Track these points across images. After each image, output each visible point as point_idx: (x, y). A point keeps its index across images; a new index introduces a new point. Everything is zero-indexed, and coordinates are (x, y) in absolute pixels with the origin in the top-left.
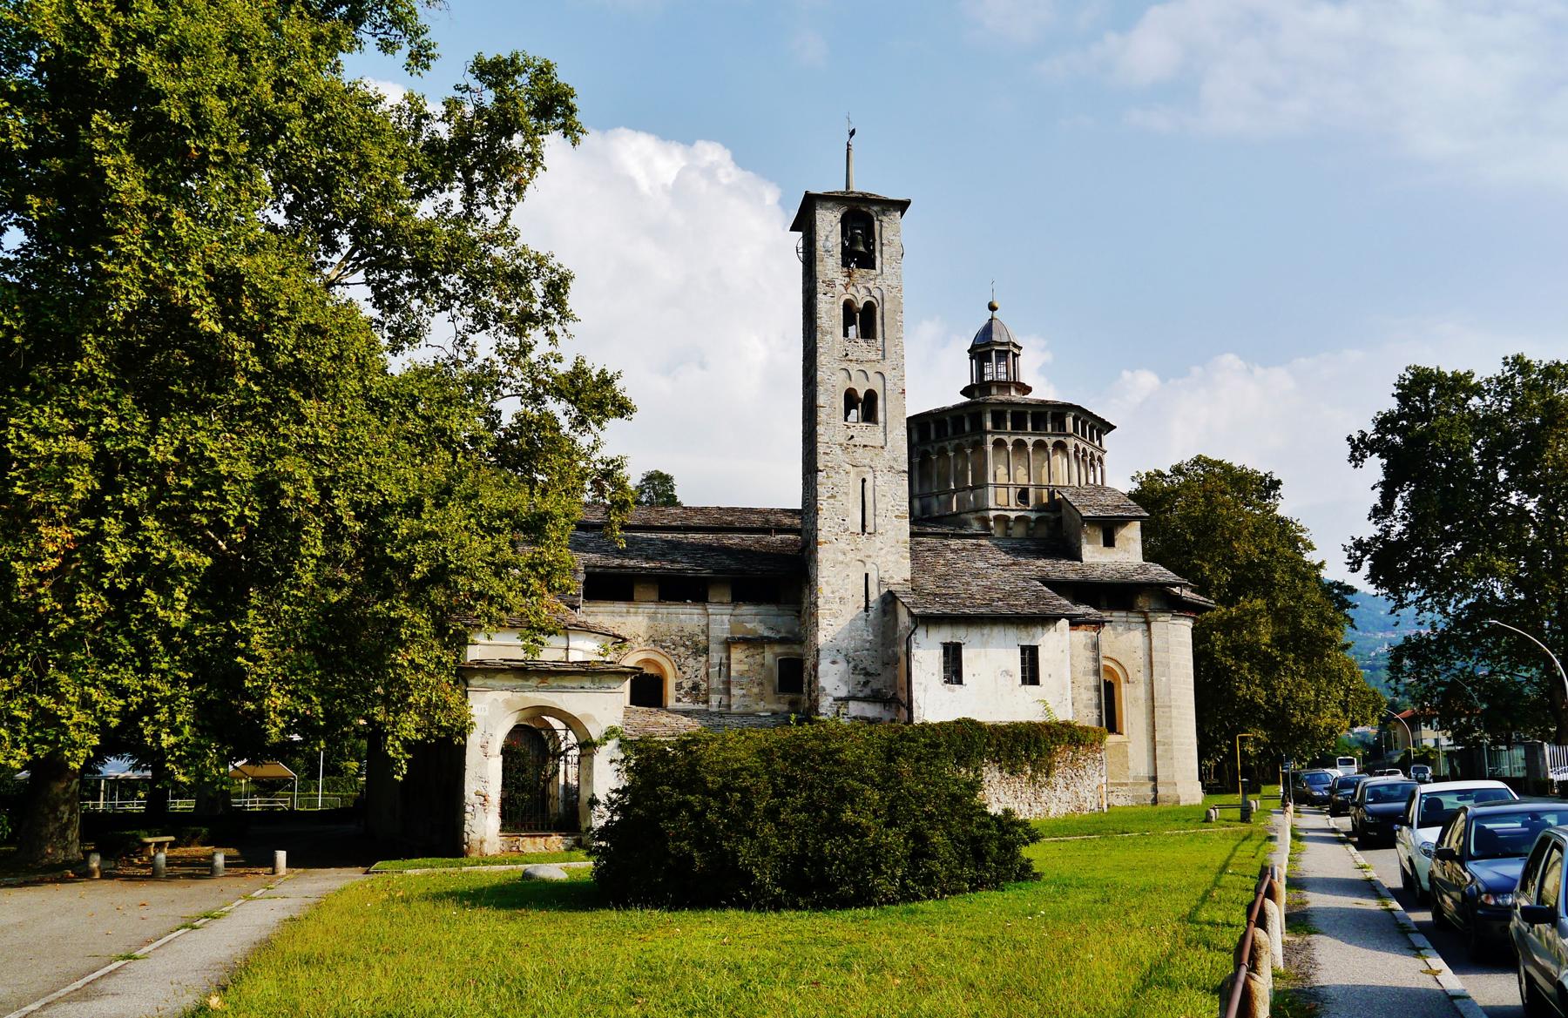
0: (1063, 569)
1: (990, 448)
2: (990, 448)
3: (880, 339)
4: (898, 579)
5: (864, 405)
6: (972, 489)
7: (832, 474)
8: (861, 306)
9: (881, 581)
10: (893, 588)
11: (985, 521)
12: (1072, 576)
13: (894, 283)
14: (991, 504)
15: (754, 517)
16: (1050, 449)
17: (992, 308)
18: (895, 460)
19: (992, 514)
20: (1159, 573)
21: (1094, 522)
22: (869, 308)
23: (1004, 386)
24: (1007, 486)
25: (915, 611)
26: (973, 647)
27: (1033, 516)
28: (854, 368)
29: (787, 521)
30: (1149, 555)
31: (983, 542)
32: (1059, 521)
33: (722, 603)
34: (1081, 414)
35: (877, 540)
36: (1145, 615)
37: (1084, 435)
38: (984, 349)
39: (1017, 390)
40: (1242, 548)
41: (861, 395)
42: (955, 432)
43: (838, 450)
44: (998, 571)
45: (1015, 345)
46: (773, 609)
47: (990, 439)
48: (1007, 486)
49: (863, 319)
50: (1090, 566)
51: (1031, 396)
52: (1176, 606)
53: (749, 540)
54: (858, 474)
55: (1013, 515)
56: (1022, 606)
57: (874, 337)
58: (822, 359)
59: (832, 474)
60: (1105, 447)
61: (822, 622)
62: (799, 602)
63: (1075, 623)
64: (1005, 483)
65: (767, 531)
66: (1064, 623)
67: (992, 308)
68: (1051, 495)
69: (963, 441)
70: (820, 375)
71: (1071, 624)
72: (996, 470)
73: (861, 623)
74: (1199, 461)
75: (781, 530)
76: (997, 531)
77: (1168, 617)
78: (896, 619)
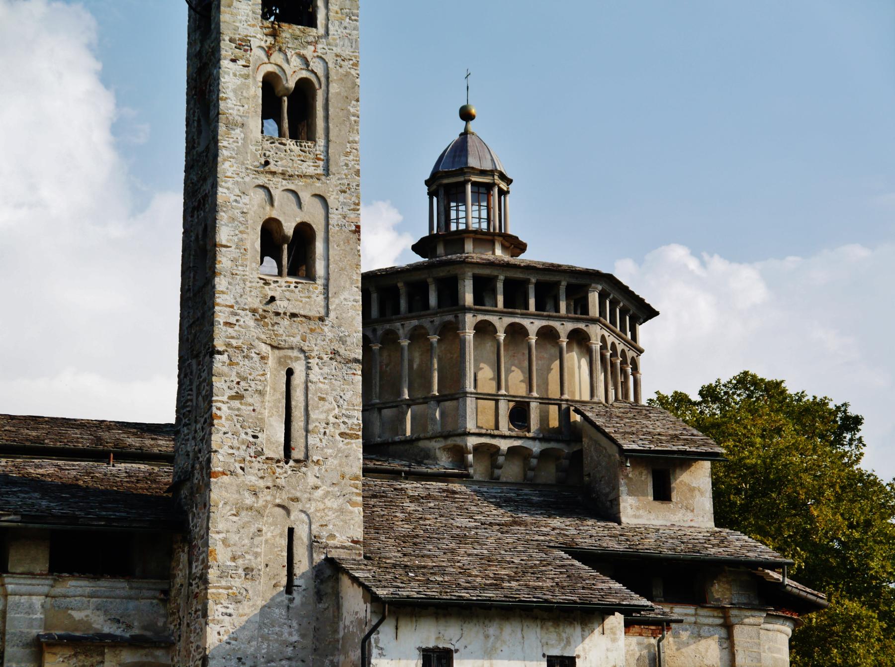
0: (592, 533)
1: (469, 334)
2: (469, 334)
3: (321, 142)
4: (341, 539)
5: (291, 250)
6: (439, 400)
7: (238, 358)
8: (291, 84)
9: (314, 543)
10: (334, 554)
11: (459, 454)
12: (613, 545)
13: (347, 52)
14: (471, 426)
15: (75, 433)
16: (564, 341)
17: (466, 115)
18: (342, 341)
19: (472, 442)
20: (741, 544)
21: (640, 458)
22: (304, 92)
23: (485, 238)
24: (495, 398)
25: (381, 592)
26: (471, 656)
27: (536, 447)
28: (278, 187)
29: (133, 441)
30: (724, 516)
31: (456, 487)
32: (577, 458)
33: (31, 575)
34: (612, 287)
35: (311, 475)
36: (724, 612)
37: (613, 322)
38: (450, 180)
39: (504, 248)
40: (823, 514)
41: (289, 229)
42: (410, 309)
43: (248, 320)
44: (493, 534)
45: (503, 177)
46: (121, 586)
47: (470, 320)
48: (495, 398)
49: (293, 108)
50: (634, 529)
51: (522, 257)
52: (771, 600)
53: (73, 470)
54: (280, 361)
55: (504, 445)
56: (547, 586)
57: (311, 137)
58: (227, 167)
59: (238, 358)
60: (642, 342)
61: (215, 610)
62: (167, 575)
63: (634, 621)
64: (491, 390)
65: (101, 456)
66: (616, 621)
67: (466, 115)
68: (564, 415)
69: (426, 322)
70: (223, 194)
71: (628, 625)
72: (479, 374)
73: (279, 613)
74: (745, 381)
75: (124, 455)
76: (477, 471)
77: (758, 618)
78: (338, 607)
